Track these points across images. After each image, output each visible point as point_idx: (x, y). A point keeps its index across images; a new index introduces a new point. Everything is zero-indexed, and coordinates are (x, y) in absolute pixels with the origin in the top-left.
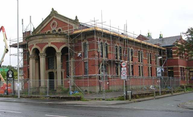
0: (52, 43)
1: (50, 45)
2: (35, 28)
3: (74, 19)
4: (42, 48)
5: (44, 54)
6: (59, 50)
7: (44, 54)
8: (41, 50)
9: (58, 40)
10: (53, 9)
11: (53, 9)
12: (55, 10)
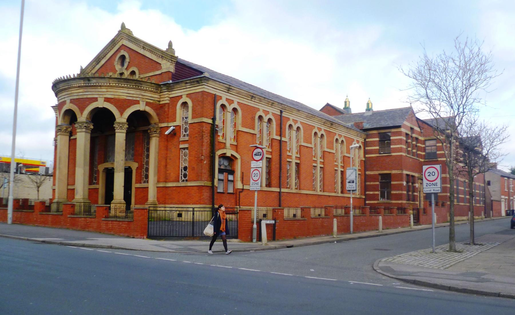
0: (107, 100)
1: (101, 104)
2: (84, 68)
3: (164, 47)
4: (82, 110)
5: (86, 123)
6: (121, 118)
7: (86, 125)
8: (80, 114)
9: (123, 93)
10: (123, 26)
11: (123, 26)
12: (127, 27)
